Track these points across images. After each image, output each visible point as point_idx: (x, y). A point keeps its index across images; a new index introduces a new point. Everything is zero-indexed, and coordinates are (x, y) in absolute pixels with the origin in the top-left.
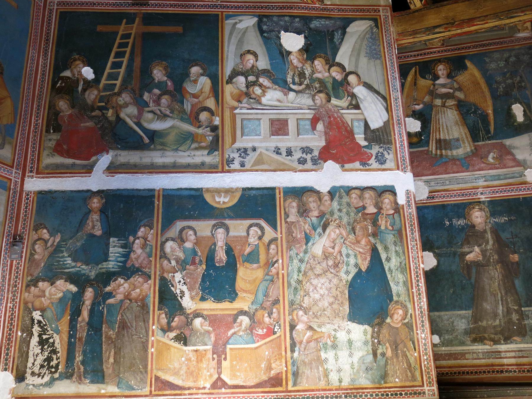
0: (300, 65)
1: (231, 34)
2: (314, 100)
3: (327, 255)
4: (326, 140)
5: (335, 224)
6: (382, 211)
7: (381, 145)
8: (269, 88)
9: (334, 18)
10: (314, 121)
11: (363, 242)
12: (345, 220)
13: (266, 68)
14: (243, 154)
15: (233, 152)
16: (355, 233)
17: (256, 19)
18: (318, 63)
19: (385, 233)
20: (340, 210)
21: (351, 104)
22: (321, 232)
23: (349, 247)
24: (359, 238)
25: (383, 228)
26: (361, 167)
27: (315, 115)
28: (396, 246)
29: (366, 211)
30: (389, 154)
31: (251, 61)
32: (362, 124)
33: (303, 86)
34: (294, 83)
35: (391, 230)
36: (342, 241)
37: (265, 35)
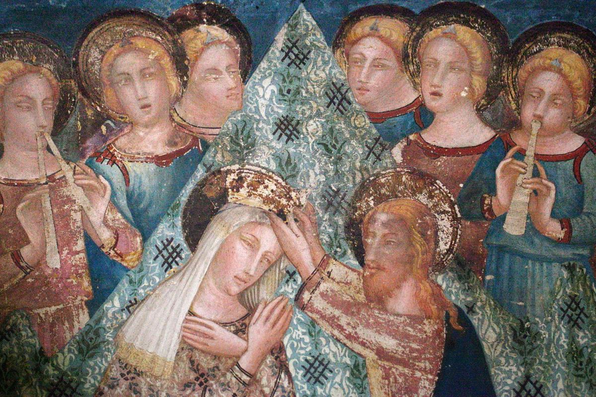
3: (206, 363)
5: (255, 202)
6: (519, 139)
11: (404, 301)
12: (314, 178)
16: (360, 253)
19: (525, 257)
20: (288, 128)
22: (180, 239)
23: (324, 326)
24: (382, 280)
25: (514, 227)
28: (574, 323)
29: (433, 137)
35: (558, 243)
36: (290, 290)
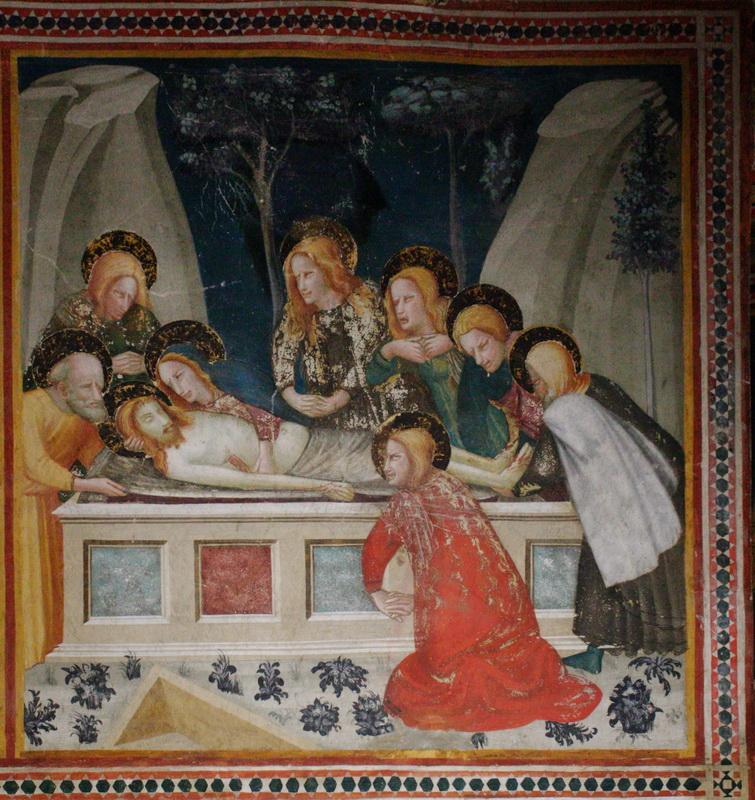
0: (329, 301)
1: (44, 155)
2: (378, 461)
4: (419, 633)
7: (641, 653)
8: (196, 406)
9: (490, 70)
10: (373, 557)
13: (187, 316)
14: (88, 690)
15: (50, 681)
17: (149, 83)
18: (411, 292)
21: (529, 476)
26: (552, 744)
27: (380, 523)
30: (667, 688)
31: (128, 286)
32: (570, 564)
33: (339, 398)
34: (302, 385)
37: (189, 157)
